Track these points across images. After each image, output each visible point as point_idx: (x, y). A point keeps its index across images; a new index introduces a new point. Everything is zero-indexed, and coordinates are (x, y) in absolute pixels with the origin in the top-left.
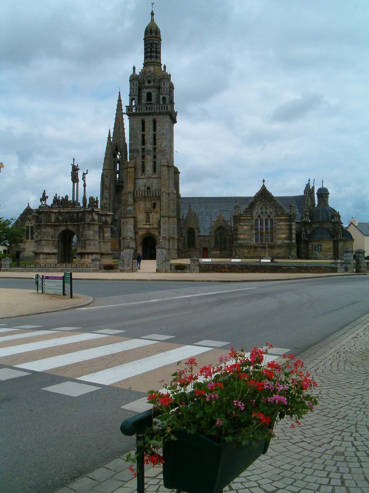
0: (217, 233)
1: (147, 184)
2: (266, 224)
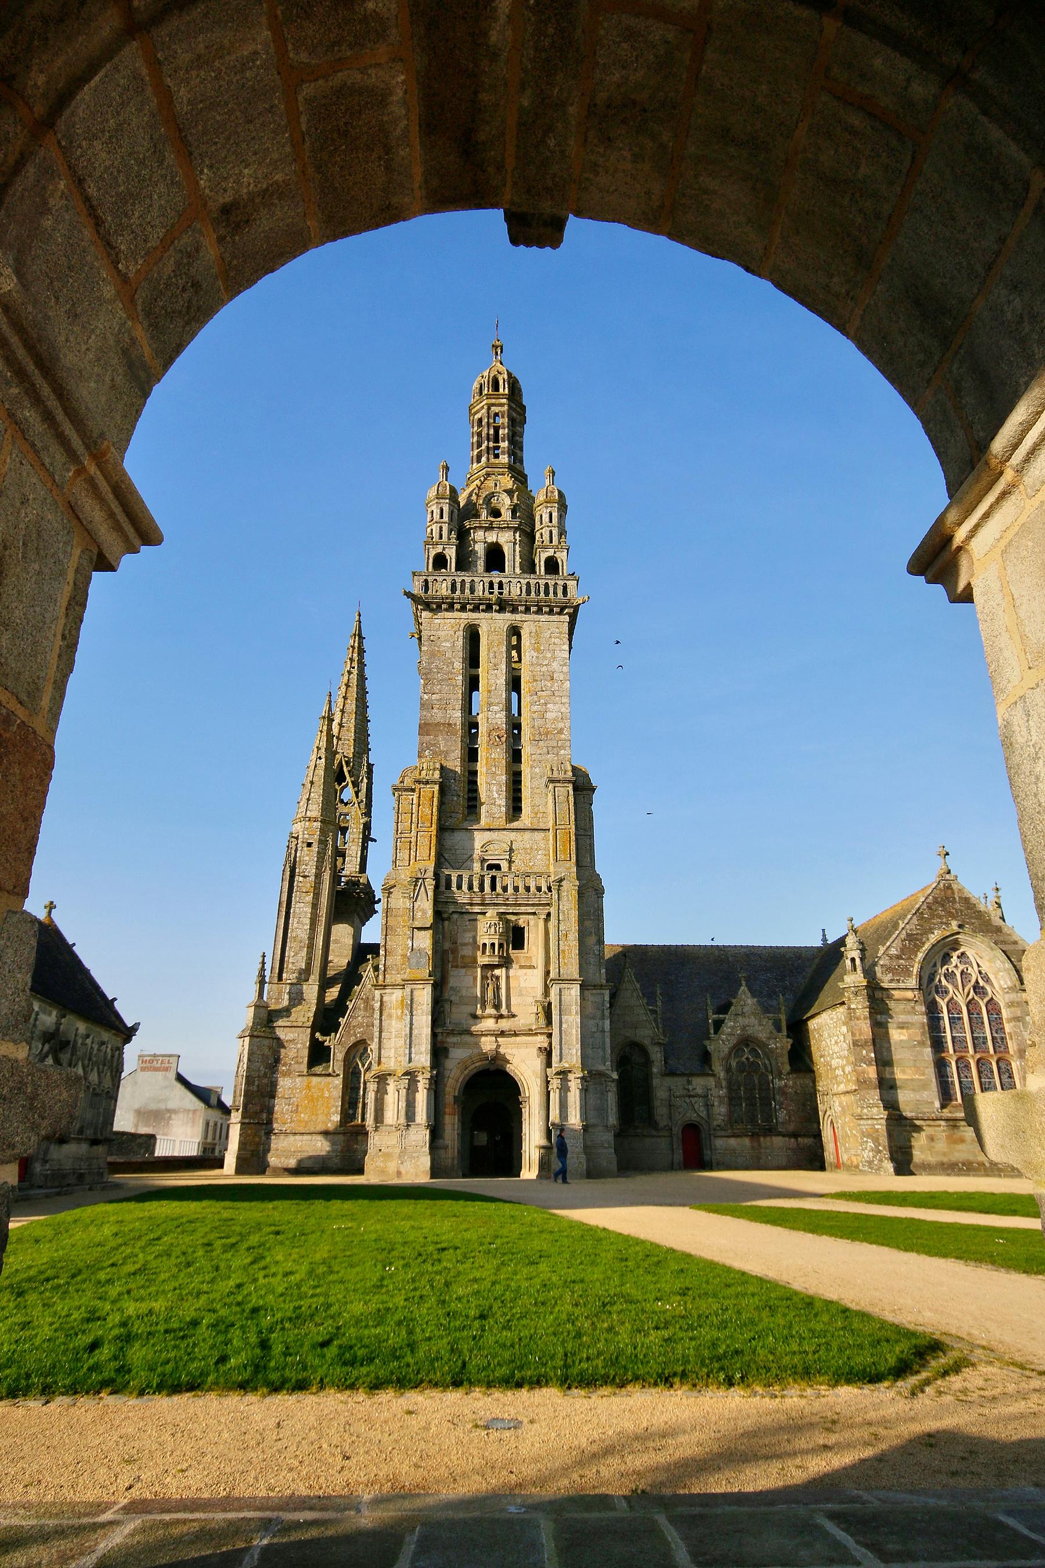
0: (734, 1064)
1: (490, 852)
2: (975, 1022)
